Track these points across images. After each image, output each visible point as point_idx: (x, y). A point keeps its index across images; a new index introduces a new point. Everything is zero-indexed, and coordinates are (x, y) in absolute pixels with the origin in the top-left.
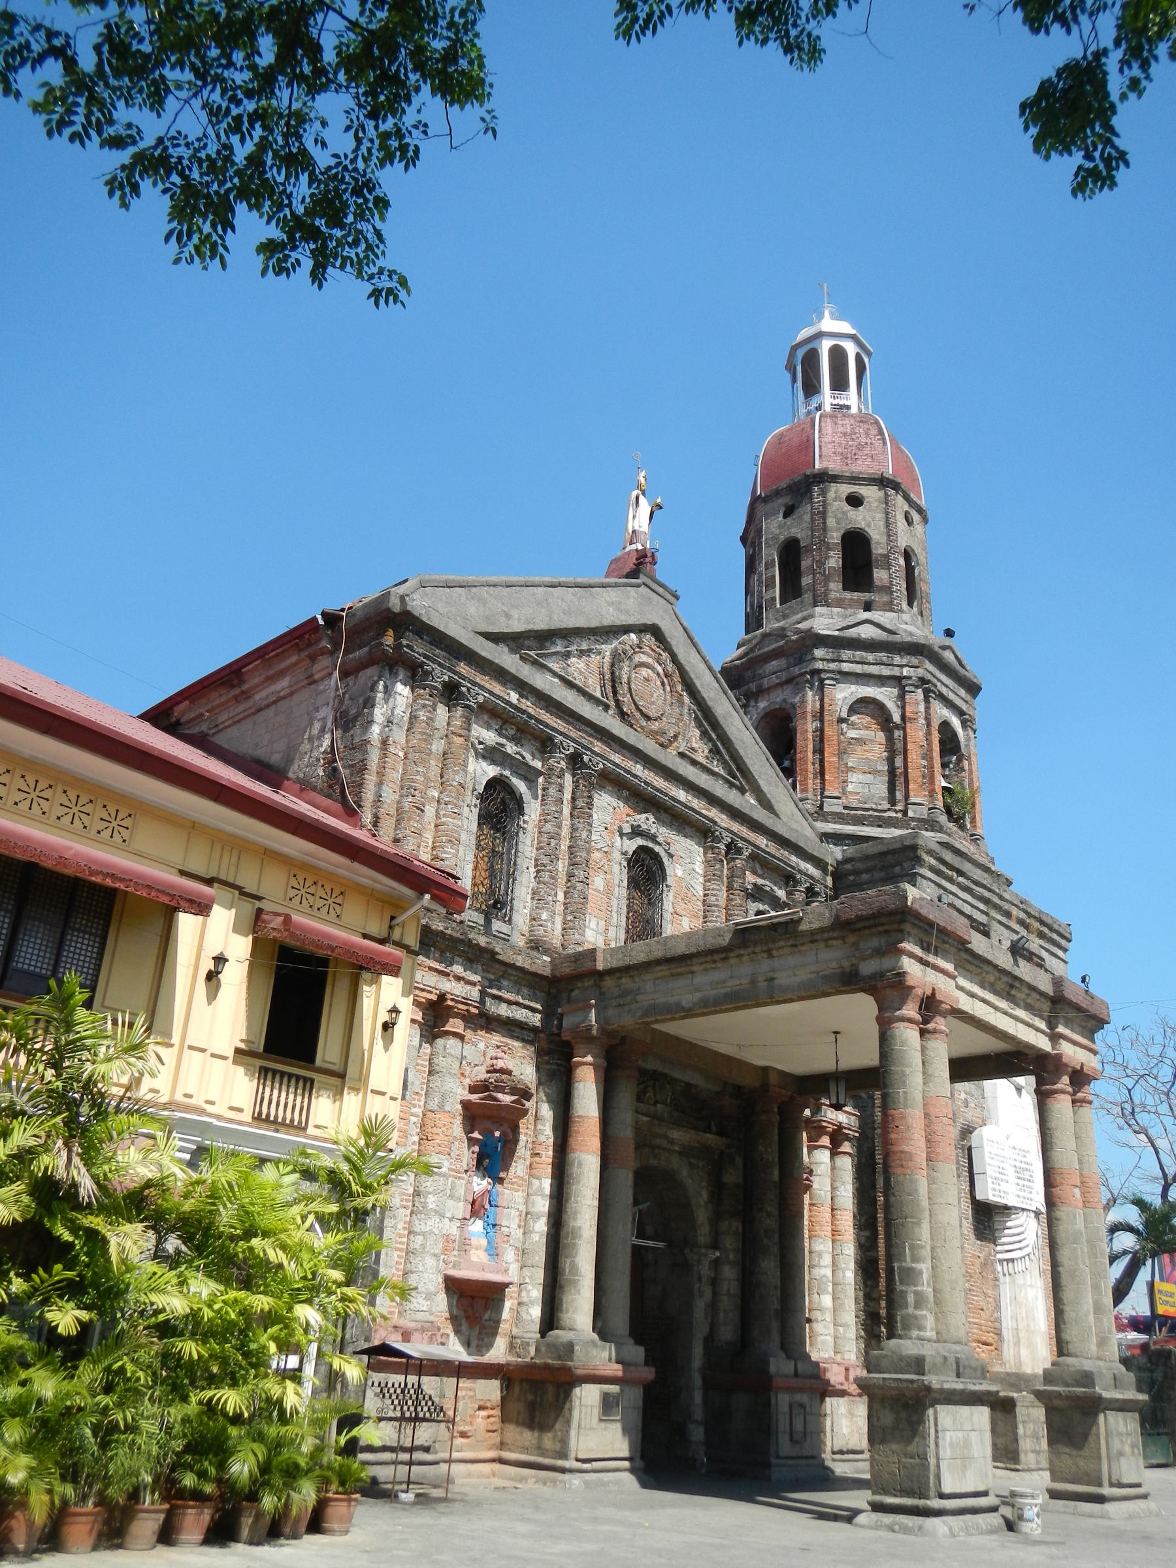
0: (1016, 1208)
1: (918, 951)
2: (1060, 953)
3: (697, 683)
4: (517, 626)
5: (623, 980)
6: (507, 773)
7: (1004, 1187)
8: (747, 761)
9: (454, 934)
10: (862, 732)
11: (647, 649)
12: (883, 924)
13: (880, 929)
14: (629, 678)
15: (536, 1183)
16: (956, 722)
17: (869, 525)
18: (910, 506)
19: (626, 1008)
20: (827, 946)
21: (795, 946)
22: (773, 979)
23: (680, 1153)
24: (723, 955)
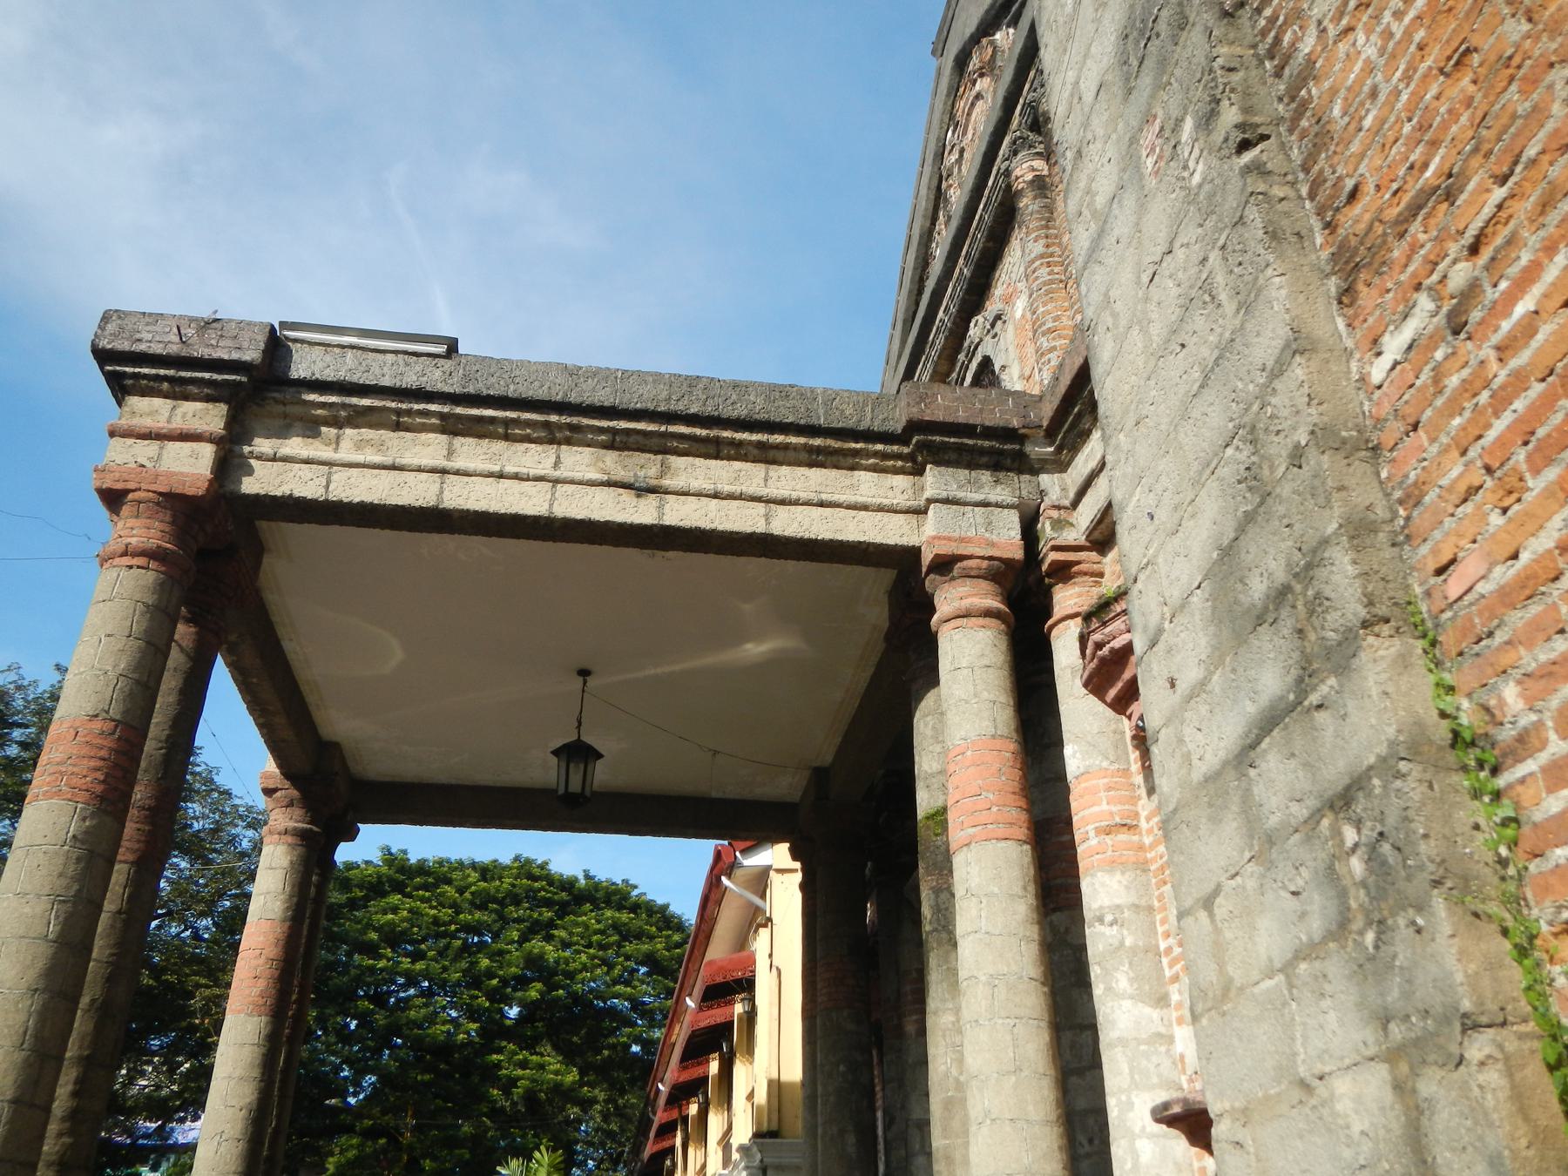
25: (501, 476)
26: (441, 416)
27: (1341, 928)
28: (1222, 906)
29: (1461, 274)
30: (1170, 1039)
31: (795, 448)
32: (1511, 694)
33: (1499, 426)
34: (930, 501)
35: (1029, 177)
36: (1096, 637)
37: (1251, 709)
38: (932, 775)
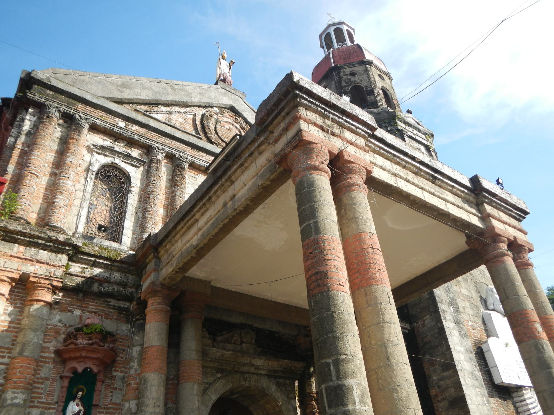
0: (525, 387)
1: (319, 120)
4: (127, 95)
5: (168, 247)
6: (117, 161)
9: (32, 233)
12: (283, 109)
13: (283, 114)
14: (215, 128)
15: (127, 405)
17: (361, 81)
18: (380, 72)
19: (170, 264)
20: (260, 154)
21: (242, 165)
22: (234, 196)
23: (269, 376)
24: (208, 197)
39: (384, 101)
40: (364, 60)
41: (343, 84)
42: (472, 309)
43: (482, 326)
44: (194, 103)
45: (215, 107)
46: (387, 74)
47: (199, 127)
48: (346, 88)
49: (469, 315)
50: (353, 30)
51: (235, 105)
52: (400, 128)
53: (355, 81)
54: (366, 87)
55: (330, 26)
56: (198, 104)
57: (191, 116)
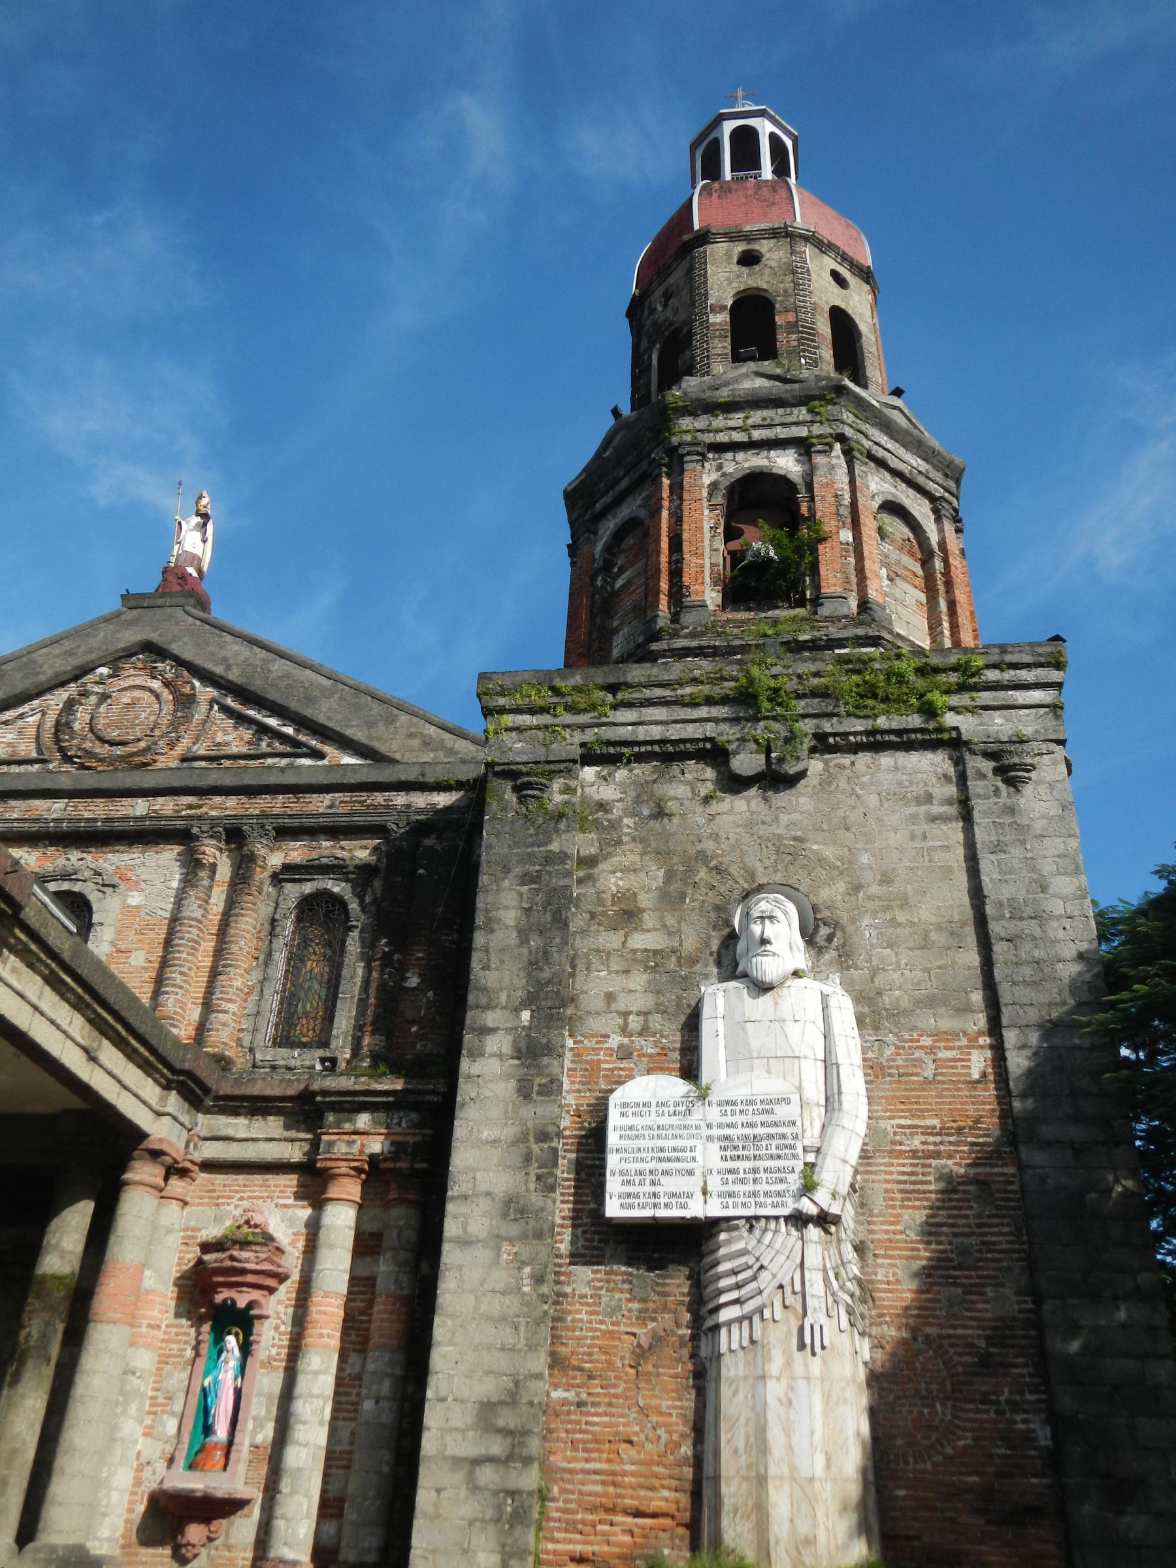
0: (728, 1219)
2: (1037, 696)
3: (219, 670)
7: (670, 1184)
8: (322, 719)
10: (628, 572)
11: (132, 672)
16: (786, 463)
25: (53, 1022)
26: (52, 971)
27: (498, 1520)
28: (445, 1494)
29: (584, 1396)
30: (136, 1441)
31: (140, 1054)
32: (556, 1489)
33: (578, 1436)
34: (168, 1114)
35: (211, 860)
36: (235, 1253)
37: (483, 1451)
38: (67, 1252)
39: (722, 346)
40: (685, 238)
41: (645, 344)
42: (658, 992)
43: (674, 1040)
44: (42, 684)
45: (103, 665)
46: (774, 234)
47: (48, 736)
48: (646, 357)
49: (625, 1015)
50: (762, 114)
51: (154, 637)
52: (675, 440)
53: (665, 321)
54: (684, 323)
55: (694, 147)
56: (54, 682)
57: (38, 717)
